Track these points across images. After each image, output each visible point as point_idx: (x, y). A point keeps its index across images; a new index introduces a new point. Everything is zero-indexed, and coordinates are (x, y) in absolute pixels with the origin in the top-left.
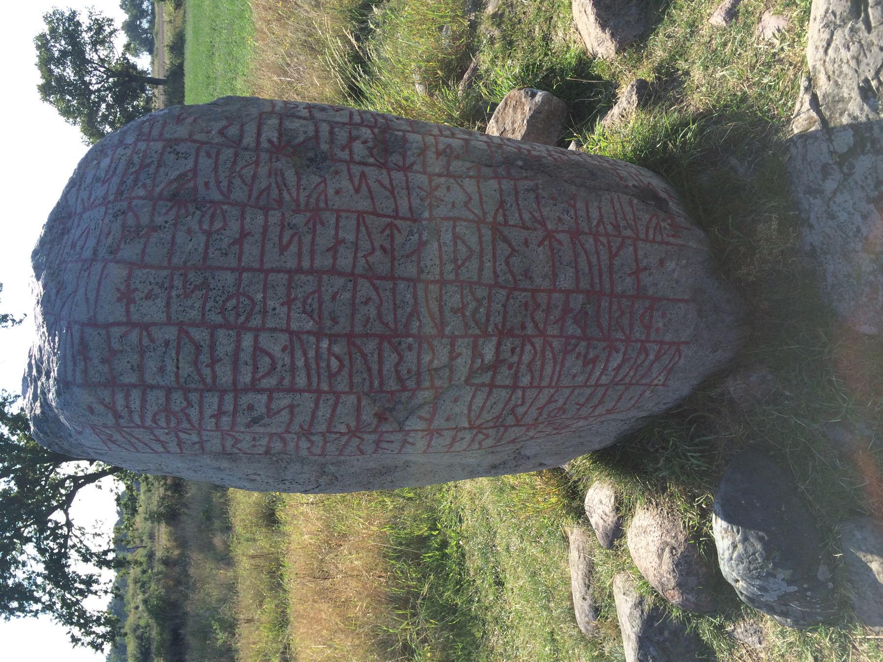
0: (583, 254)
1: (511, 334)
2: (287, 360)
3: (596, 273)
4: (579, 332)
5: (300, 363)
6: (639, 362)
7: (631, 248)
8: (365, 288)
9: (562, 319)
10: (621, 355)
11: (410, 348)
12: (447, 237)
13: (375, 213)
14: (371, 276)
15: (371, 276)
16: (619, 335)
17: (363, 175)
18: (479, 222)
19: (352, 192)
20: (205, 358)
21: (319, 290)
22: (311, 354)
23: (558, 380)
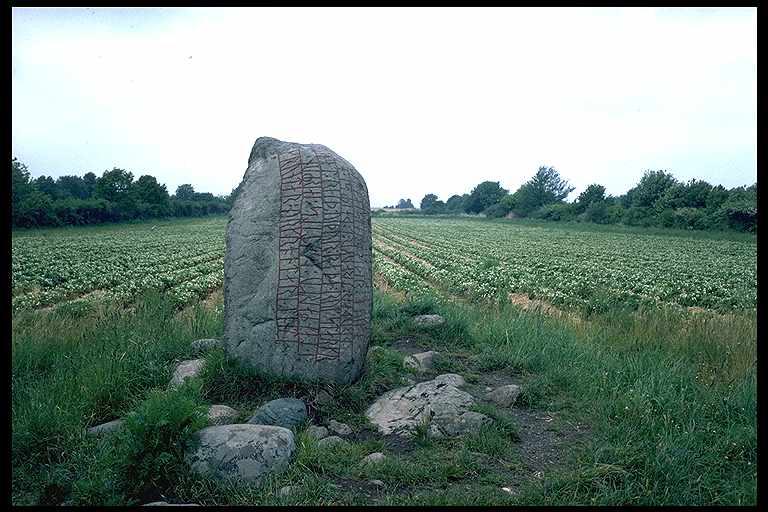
5: (333, 216)
14: (355, 238)
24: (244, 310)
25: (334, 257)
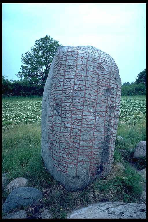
0: (87, 148)
1: (71, 130)
2: (69, 84)
4: (71, 146)
5: (68, 87)
7: (88, 161)
8: (82, 99)
9: (74, 142)
11: (70, 108)
12: (92, 118)
13: (97, 104)
15: (85, 101)
17: (105, 102)
18: (95, 125)
19: (101, 99)
20: (70, 70)
21: (81, 90)
22: (70, 89)
23: (61, 142)
25: (67, 112)
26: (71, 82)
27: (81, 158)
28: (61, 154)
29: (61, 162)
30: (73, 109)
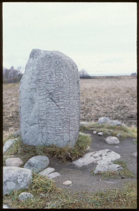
3: (72, 123)
6: (60, 133)
9: (66, 118)
10: (61, 129)
11: (62, 95)
16: (64, 128)
22: (61, 82)
24: (26, 120)
25: (61, 98)
26: (61, 78)
27: (71, 128)
28: (57, 128)
29: (58, 133)
30: (65, 96)
